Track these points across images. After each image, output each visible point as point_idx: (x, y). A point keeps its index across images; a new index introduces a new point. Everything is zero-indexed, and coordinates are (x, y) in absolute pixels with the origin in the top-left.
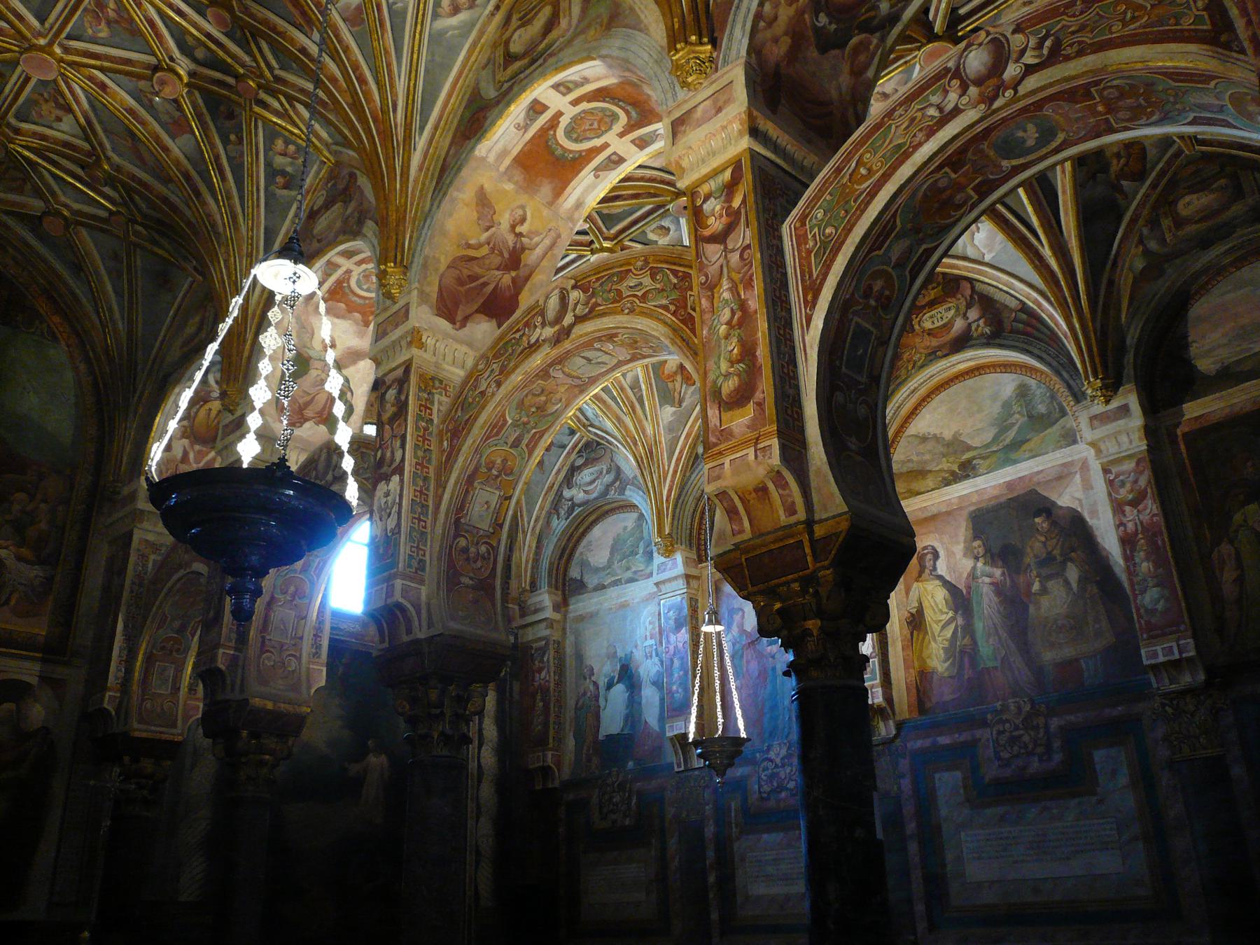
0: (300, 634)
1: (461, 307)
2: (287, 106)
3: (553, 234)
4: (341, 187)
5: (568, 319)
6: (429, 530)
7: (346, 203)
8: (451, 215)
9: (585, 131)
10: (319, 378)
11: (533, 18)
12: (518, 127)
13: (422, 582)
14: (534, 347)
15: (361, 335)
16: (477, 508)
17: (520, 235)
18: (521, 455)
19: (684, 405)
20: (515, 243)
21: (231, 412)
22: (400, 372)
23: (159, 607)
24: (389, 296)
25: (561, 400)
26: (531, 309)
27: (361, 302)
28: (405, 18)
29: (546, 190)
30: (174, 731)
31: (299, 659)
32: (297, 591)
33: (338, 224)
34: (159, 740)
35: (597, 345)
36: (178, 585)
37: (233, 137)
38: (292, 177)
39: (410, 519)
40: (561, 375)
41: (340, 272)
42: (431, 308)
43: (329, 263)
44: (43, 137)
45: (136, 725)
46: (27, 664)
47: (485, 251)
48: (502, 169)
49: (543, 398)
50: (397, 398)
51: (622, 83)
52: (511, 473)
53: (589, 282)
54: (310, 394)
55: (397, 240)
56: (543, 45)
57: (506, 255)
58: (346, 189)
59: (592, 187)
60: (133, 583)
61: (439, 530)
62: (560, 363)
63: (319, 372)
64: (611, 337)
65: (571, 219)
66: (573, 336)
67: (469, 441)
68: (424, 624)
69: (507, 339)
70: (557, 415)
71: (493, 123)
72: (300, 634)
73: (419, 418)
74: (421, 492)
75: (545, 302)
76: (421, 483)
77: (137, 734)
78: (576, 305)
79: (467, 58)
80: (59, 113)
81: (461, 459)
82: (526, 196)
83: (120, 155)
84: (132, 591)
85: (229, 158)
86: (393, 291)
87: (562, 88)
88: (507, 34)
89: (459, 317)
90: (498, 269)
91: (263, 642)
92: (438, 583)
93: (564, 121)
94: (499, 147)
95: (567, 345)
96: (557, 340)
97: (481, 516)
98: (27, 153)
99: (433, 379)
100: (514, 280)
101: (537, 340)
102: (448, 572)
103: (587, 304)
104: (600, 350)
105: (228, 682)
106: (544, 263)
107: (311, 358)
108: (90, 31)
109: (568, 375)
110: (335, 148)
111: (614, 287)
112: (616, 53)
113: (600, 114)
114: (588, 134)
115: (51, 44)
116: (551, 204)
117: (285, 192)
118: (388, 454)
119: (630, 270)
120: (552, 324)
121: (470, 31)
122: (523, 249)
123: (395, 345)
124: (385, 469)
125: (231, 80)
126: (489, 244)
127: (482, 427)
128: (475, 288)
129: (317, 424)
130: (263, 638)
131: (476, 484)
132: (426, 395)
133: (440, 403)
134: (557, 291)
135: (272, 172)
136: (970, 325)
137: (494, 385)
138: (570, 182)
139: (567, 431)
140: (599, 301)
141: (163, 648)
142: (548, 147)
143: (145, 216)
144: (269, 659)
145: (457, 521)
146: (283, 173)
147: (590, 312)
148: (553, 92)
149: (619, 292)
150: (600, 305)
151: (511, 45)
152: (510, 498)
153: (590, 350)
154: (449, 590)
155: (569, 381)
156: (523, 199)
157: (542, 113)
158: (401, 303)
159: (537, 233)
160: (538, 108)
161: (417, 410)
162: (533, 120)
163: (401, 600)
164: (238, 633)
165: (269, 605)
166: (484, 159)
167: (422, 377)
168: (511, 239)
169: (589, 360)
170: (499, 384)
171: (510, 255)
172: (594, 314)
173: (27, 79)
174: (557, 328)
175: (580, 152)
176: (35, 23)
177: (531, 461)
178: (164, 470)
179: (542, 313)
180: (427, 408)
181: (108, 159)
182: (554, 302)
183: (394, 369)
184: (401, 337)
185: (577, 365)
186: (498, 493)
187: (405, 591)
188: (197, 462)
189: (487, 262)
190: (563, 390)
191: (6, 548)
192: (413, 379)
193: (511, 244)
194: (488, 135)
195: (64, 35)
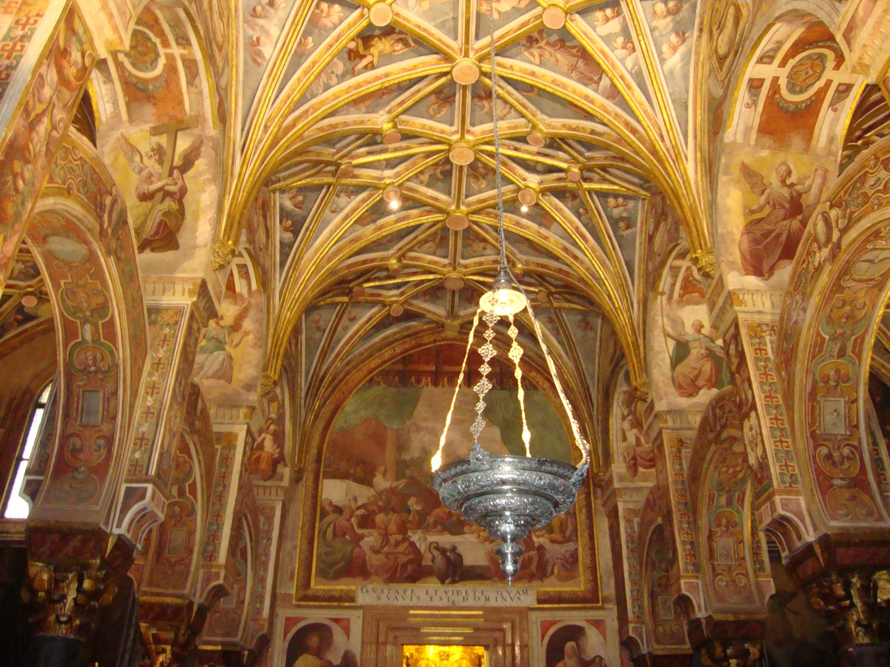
0: (742, 555)
1: (765, 261)
2: (602, 173)
3: (820, 172)
4: (660, 211)
5: (836, 235)
6: (791, 448)
7: (665, 220)
8: (728, 195)
9: (804, 80)
11: (725, 23)
12: (748, 106)
13: (797, 493)
14: (819, 270)
16: (828, 418)
17: (792, 185)
18: (850, 361)
20: (791, 193)
21: (645, 401)
22: (732, 329)
23: (648, 555)
24: (707, 275)
25: (865, 304)
26: (808, 239)
28: (643, 75)
30: (684, 647)
31: (746, 575)
32: (728, 522)
33: (666, 238)
34: (676, 656)
35: (870, 246)
36: (654, 538)
37: (581, 210)
38: (629, 219)
39: (772, 443)
40: (854, 283)
41: (683, 271)
42: (739, 271)
43: (672, 268)
44: (481, 264)
45: (656, 646)
46: (576, 613)
47: (767, 210)
48: (752, 142)
49: (848, 308)
50: (737, 350)
51: (809, 28)
52: (848, 380)
53: (840, 197)
55: (698, 231)
56: (738, 37)
57: (787, 206)
58: (663, 210)
59: (836, 120)
60: (627, 542)
61: (801, 445)
62: (846, 273)
63: (698, 349)
64: (877, 235)
65: (830, 153)
66: (843, 247)
67: (798, 366)
68: (810, 528)
69: (799, 270)
70: (868, 317)
71: (729, 114)
72: (742, 555)
73: (757, 360)
74: (776, 419)
75: (815, 229)
76: (775, 412)
77: (659, 653)
78: (837, 221)
79: (696, 77)
80: (482, 245)
81: (797, 382)
82: (782, 154)
83: (525, 254)
84: (628, 548)
85: (584, 225)
86: (708, 270)
87: (765, 60)
88: (714, 44)
89: (766, 268)
90: (784, 219)
91: (714, 569)
92: (812, 490)
93: (783, 83)
94: (741, 127)
95: (843, 257)
96: (833, 256)
97: (834, 424)
98: (476, 278)
99: (759, 325)
101: (820, 263)
102: (818, 479)
103: (844, 216)
104: (874, 249)
105: (695, 604)
107: (688, 342)
108: (476, 187)
109: (861, 281)
110: (646, 185)
111: (860, 192)
112: (784, 9)
113: (809, 62)
114: (808, 82)
115: (458, 207)
116: (806, 150)
117: (628, 231)
118: (743, 396)
119: (867, 172)
120: (826, 246)
121: (690, 59)
122: (800, 195)
123: (723, 310)
124: (745, 409)
125: (562, 175)
126: (769, 203)
127: (805, 350)
128: (772, 240)
129: (709, 389)
130: (713, 564)
131: (819, 398)
132: (758, 340)
133: (772, 342)
134: (820, 217)
135: (614, 222)
137: (801, 313)
138: (815, 125)
140: (853, 209)
141: (660, 585)
142: (780, 108)
143: (556, 287)
144: (722, 580)
145: (813, 434)
146: (622, 219)
147: (850, 220)
148: (761, 67)
149: (865, 195)
150: (854, 213)
151: (719, 50)
152: (856, 401)
153: (866, 252)
154: (823, 494)
155: (864, 285)
156: (781, 157)
157: (761, 86)
158: (716, 277)
159: (807, 177)
160: (755, 84)
161: (753, 354)
162: (757, 95)
163: (783, 513)
164: (694, 564)
165: (710, 537)
166: (734, 142)
167: (749, 327)
168: (786, 192)
169: (871, 261)
170: (804, 310)
171: (790, 203)
172: (853, 221)
173: (456, 233)
174: (830, 246)
175: (810, 98)
176: (443, 197)
177: (863, 363)
178: (625, 454)
179: (816, 240)
180: (761, 350)
181: (519, 260)
182: (821, 227)
183: (728, 330)
184: (724, 302)
185: (862, 269)
186: (842, 399)
187: (785, 505)
188: (647, 443)
189: (773, 218)
190: (862, 295)
191: (543, 536)
192: (743, 332)
194: (728, 123)
195: (463, 197)
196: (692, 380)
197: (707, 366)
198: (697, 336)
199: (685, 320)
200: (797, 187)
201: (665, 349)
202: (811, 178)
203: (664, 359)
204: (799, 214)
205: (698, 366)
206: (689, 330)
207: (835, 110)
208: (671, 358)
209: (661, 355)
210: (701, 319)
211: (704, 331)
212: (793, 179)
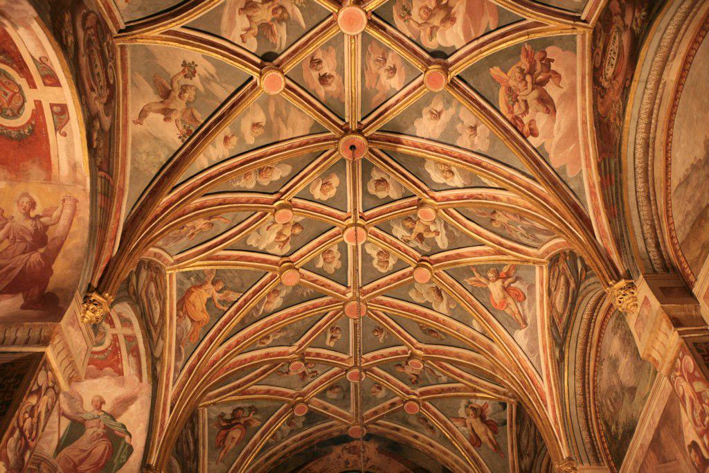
3: (68, 202)
10: (95, 434)
15: (122, 383)
17: (38, 217)
19: (529, 321)
20: (36, 225)
27: (101, 356)
29: (35, 170)
54: (85, 451)
57: (29, 239)
59: (70, 146)
63: (95, 429)
82: (22, 184)
90: (24, 253)
100: (42, 255)
106: (74, 228)
107: (85, 420)
116: (49, 179)
122: (46, 227)
126: (8, 238)
136: (631, 28)
139: (500, 407)
156: (21, 188)
171: (33, 236)
175: (29, 122)
193: (31, 228)
196: (75, 463)
197: (101, 448)
198: (96, 413)
199: (83, 396)
200: (42, 220)
201: (57, 430)
202: (59, 209)
203: (51, 441)
204: (41, 247)
205: (89, 447)
206: (88, 407)
207: (65, 135)
208: (60, 441)
209: (49, 438)
210: (102, 395)
211: (104, 408)
212: (39, 210)
